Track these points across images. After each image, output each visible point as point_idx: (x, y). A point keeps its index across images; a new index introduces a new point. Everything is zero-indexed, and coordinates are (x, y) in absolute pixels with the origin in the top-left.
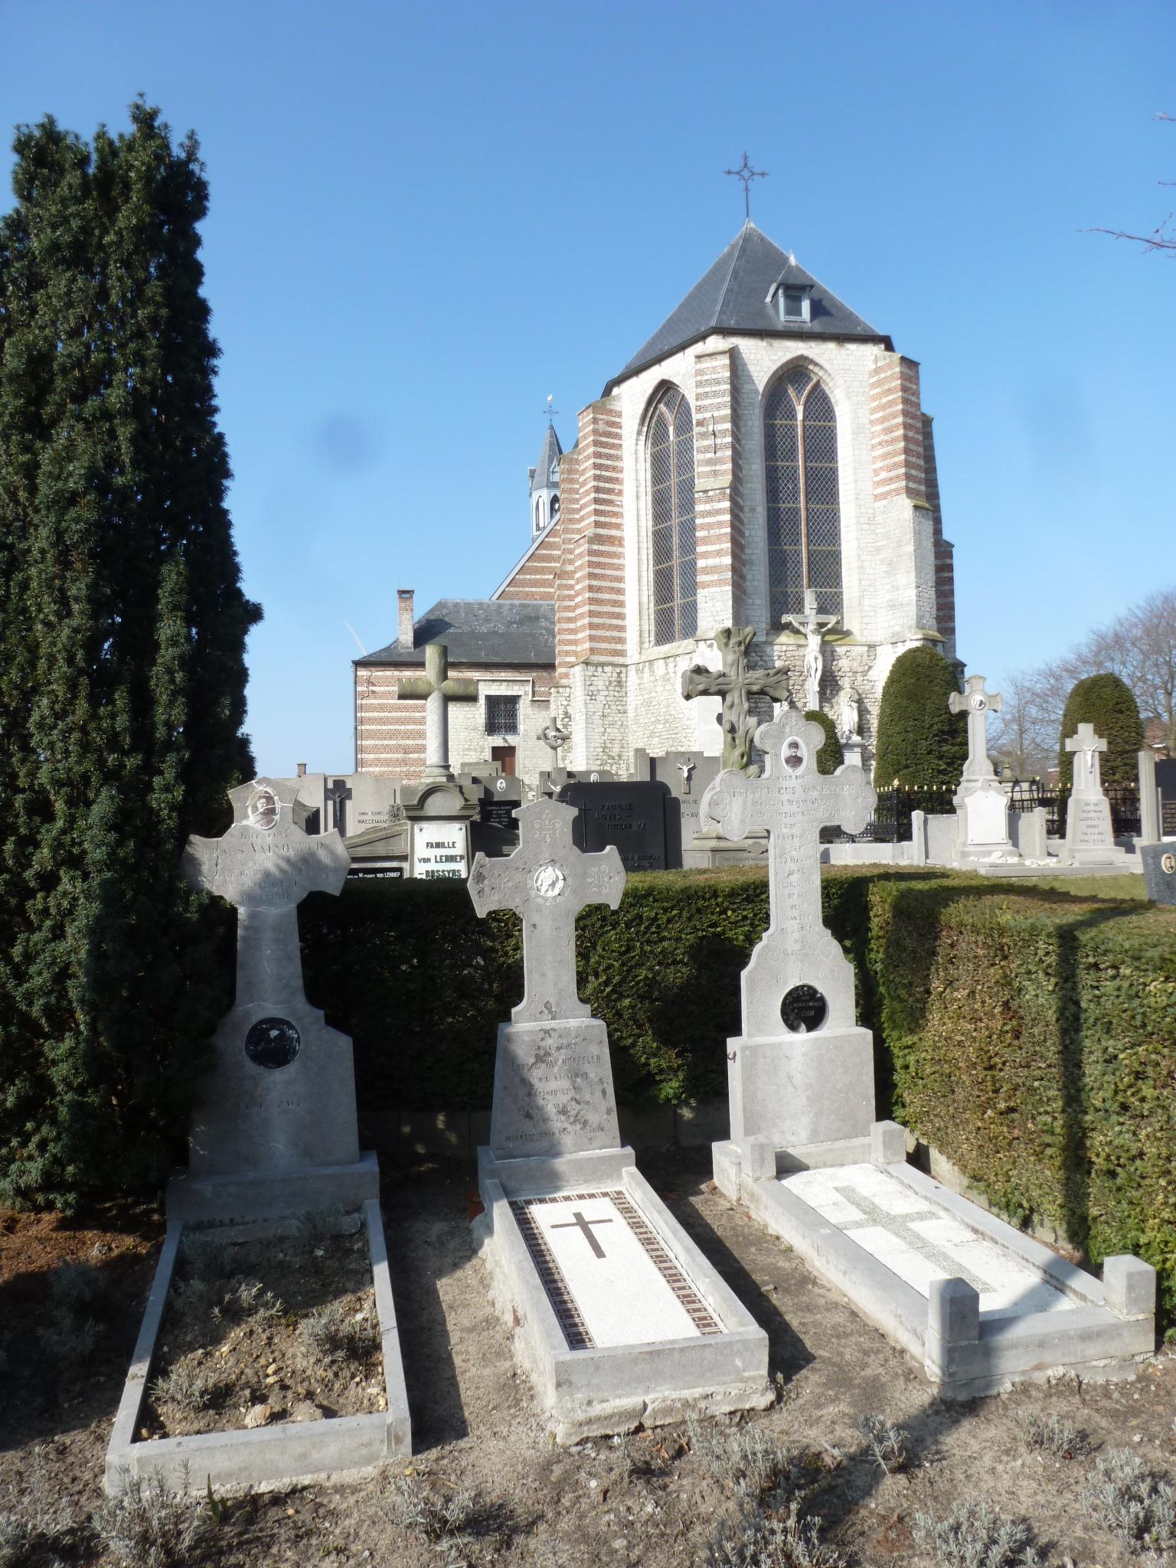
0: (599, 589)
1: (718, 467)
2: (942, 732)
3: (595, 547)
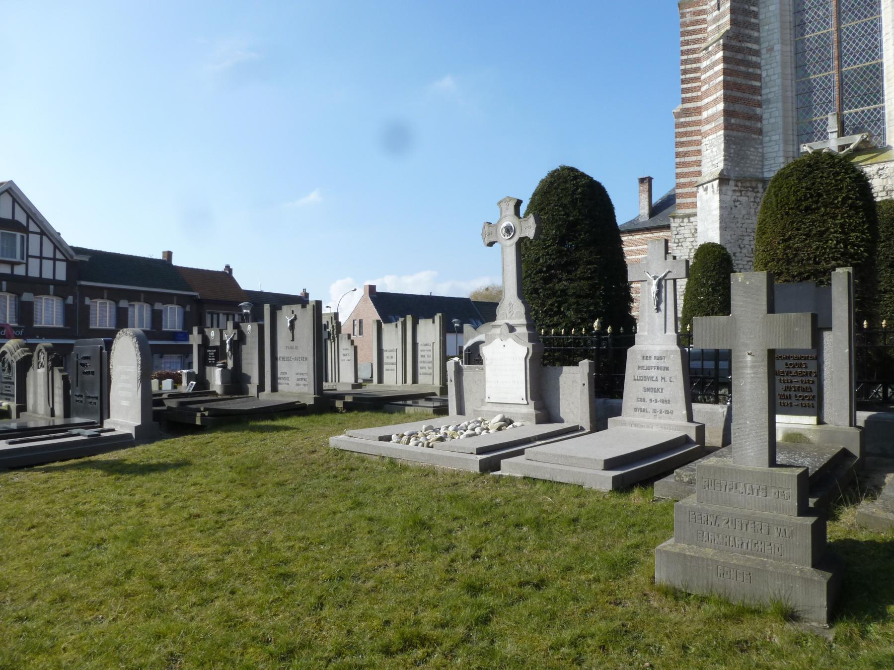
0: (686, 154)
1: (720, 23)
2: (550, 268)
3: (682, 120)
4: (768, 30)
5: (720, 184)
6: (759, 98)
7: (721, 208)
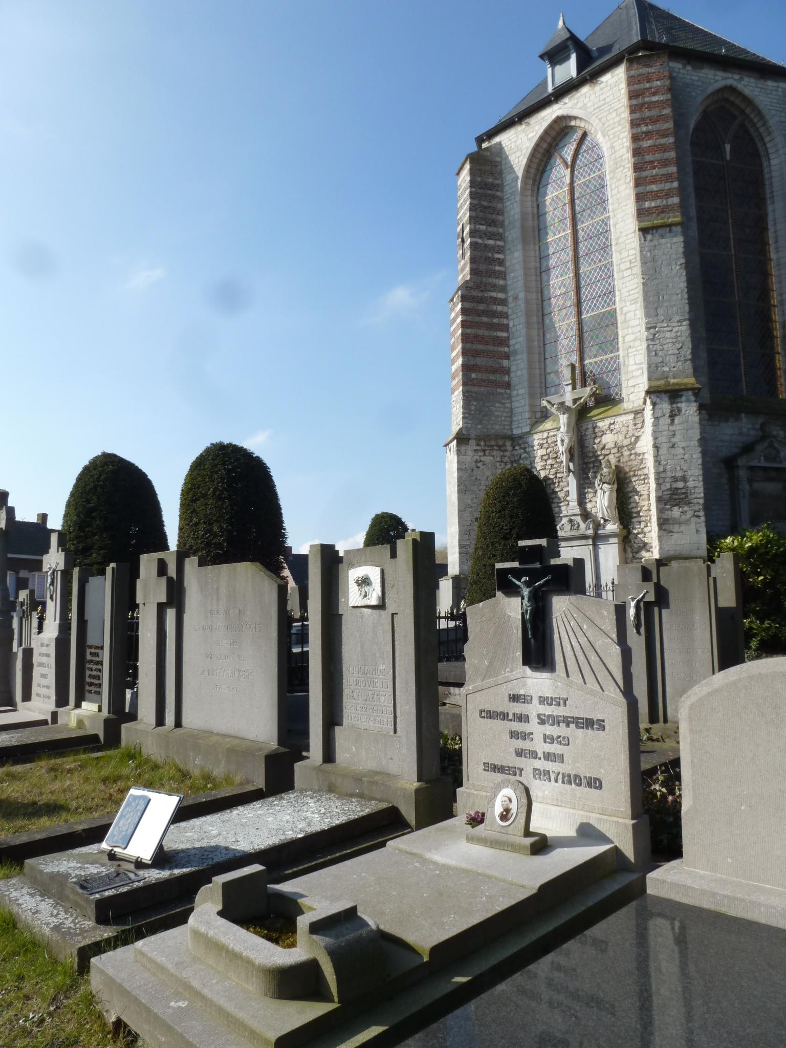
4: (514, 278)
5: (458, 444)
6: (506, 349)
7: (459, 469)
